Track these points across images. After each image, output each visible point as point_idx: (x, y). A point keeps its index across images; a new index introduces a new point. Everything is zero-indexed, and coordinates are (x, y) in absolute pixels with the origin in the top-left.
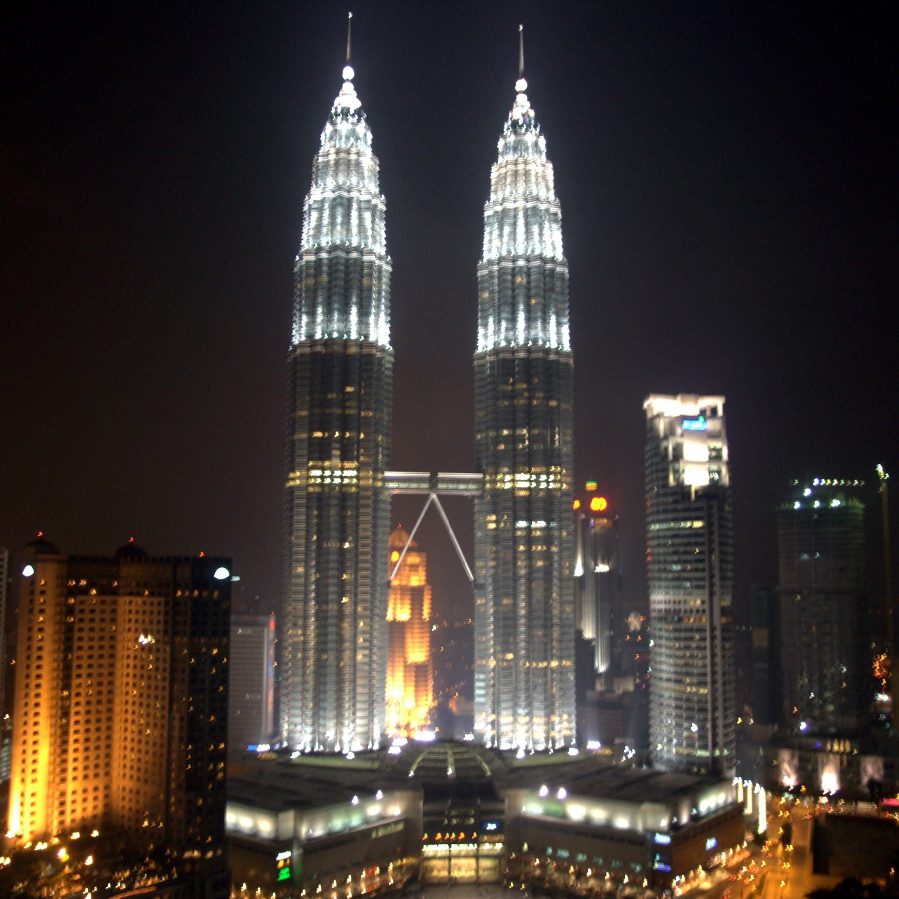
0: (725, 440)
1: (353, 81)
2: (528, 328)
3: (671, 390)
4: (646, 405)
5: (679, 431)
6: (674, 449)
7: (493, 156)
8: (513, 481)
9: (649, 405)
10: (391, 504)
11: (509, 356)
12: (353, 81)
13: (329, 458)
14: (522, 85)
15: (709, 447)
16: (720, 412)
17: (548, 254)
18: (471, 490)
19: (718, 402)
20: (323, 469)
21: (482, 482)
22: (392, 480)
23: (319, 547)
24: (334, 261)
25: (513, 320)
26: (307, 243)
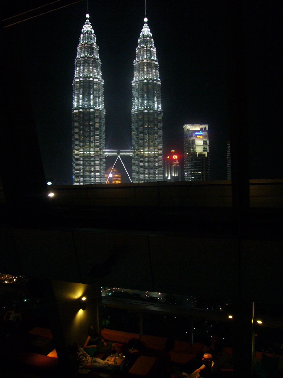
0: (208, 138)
1: (89, 19)
2: (148, 102)
3: (192, 123)
4: (184, 127)
5: (194, 135)
6: (192, 141)
7: (137, 44)
8: (144, 151)
9: (185, 127)
10: (106, 159)
11: (142, 112)
12: (89, 19)
13: (86, 145)
14: (146, 20)
15: (203, 140)
16: (207, 129)
17: (154, 77)
18: (131, 154)
19: (206, 126)
20: (83, 149)
21: (134, 152)
22: (106, 152)
23: (84, 173)
24: (85, 81)
25: (143, 100)
26: (76, 75)
